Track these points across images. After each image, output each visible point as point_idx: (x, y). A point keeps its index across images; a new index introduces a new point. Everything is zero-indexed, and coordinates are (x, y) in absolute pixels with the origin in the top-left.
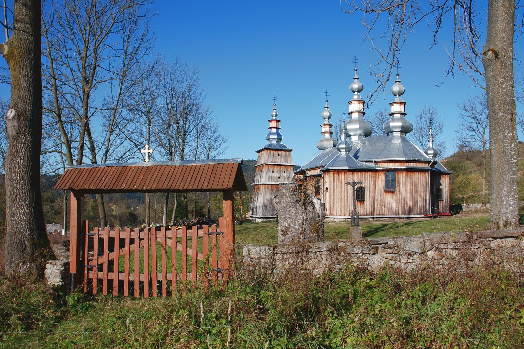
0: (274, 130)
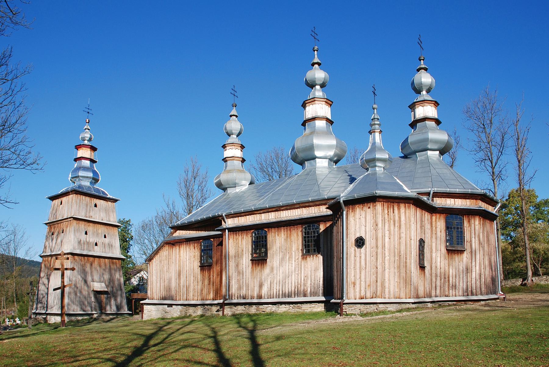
0: (87, 163)
